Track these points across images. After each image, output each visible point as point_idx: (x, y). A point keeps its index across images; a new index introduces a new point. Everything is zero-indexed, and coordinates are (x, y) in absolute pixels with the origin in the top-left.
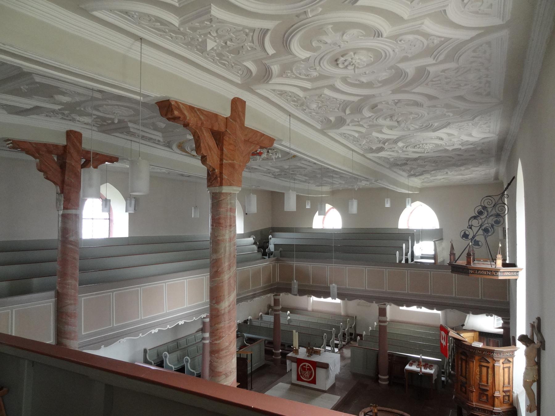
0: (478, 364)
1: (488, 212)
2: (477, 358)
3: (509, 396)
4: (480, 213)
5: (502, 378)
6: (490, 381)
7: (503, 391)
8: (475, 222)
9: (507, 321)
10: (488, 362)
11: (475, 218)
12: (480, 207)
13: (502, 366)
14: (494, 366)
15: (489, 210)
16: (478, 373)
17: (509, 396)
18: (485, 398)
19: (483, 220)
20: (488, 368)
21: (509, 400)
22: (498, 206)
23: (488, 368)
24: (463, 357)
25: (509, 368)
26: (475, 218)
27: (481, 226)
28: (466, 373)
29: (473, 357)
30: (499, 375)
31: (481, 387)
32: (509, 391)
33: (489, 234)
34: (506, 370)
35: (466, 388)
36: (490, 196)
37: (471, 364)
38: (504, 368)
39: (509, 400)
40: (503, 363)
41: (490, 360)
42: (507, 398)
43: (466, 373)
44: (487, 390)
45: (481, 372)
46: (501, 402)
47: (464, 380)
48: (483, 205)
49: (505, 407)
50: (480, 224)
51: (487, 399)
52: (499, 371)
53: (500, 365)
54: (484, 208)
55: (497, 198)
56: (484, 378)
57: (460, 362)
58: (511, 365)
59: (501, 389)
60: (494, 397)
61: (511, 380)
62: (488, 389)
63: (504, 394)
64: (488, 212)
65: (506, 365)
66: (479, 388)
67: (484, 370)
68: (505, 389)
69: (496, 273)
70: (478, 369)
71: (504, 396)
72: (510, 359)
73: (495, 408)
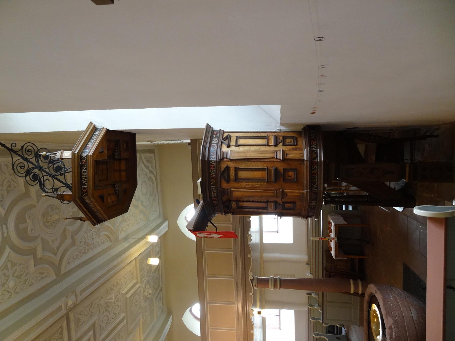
0: (236, 185)
1: (33, 168)
2: (225, 185)
3: (284, 138)
4: (35, 178)
5: (253, 148)
6: (260, 165)
7: (276, 145)
8: (48, 185)
10: (228, 168)
11: (42, 185)
12: (28, 178)
13: (233, 148)
14: (231, 160)
15: (31, 166)
16: (251, 183)
17: (284, 138)
18: (290, 173)
19: (44, 174)
20: (237, 169)
21: (292, 137)
23: (237, 169)
24: (234, 205)
25: (237, 138)
26: (42, 185)
27: (53, 177)
29: (224, 192)
30: (246, 152)
32: (276, 138)
33: (63, 166)
34: (241, 142)
38: (237, 145)
39: (292, 137)
40: (229, 146)
41: (223, 166)
42: (288, 141)
44: (276, 170)
45: (247, 180)
46: (295, 150)
48: (24, 175)
49: (302, 142)
50: (50, 178)
52: (239, 152)
53: (233, 152)
54: (28, 172)
56: (257, 174)
58: (234, 136)
59: (273, 149)
61: (254, 135)
62: (273, 169)
63: (281, 144)
64: (33, 168)
65: (233, 142)
67: (242, 174)
68: (272, 142)
69: (84, 159)
70: (244, 184)
71: (284, 145)
72: (225, 135)
73: (305, 158)
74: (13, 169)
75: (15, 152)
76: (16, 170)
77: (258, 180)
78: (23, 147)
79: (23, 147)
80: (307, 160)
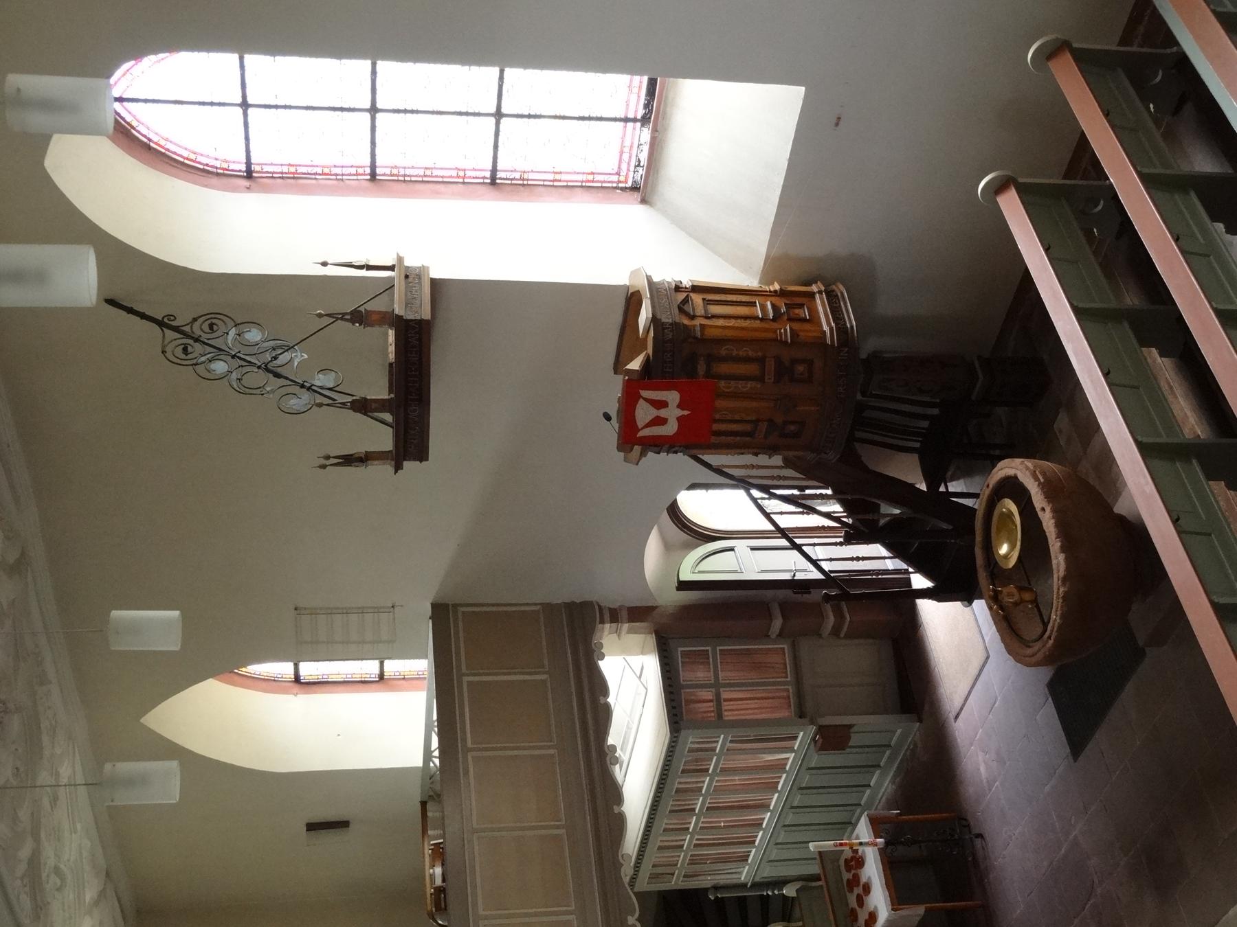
2: (686, 322)
9: (607, 616)
14: (696, 289)
18: (797, 311)
22: (198, 332)
24: (701, 368)
28: (747, 360)
31: (771, 315)
35: (794, 361)
36: (164, 347)
37: (711, 333)
43: (747, 360)
47: (771, 365)
51: (801, 306)
55: (170, 334)
57: (722, 383)
60: (782, 293)
66: (774, 320)
74: (164, 352)
75: (176, 329)
76: (169, 355)
77: (745, 318)
78: (195, 320)
79: (195, 320)
80: (820, 292)
